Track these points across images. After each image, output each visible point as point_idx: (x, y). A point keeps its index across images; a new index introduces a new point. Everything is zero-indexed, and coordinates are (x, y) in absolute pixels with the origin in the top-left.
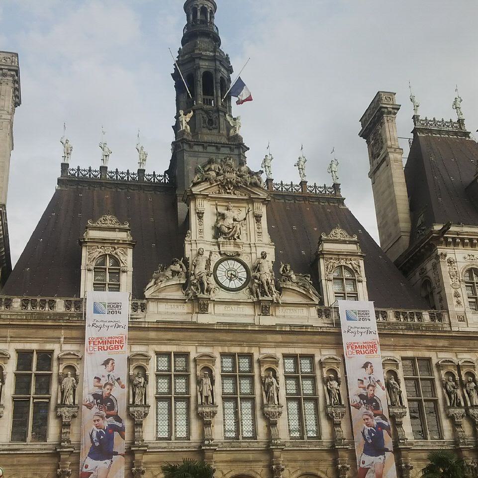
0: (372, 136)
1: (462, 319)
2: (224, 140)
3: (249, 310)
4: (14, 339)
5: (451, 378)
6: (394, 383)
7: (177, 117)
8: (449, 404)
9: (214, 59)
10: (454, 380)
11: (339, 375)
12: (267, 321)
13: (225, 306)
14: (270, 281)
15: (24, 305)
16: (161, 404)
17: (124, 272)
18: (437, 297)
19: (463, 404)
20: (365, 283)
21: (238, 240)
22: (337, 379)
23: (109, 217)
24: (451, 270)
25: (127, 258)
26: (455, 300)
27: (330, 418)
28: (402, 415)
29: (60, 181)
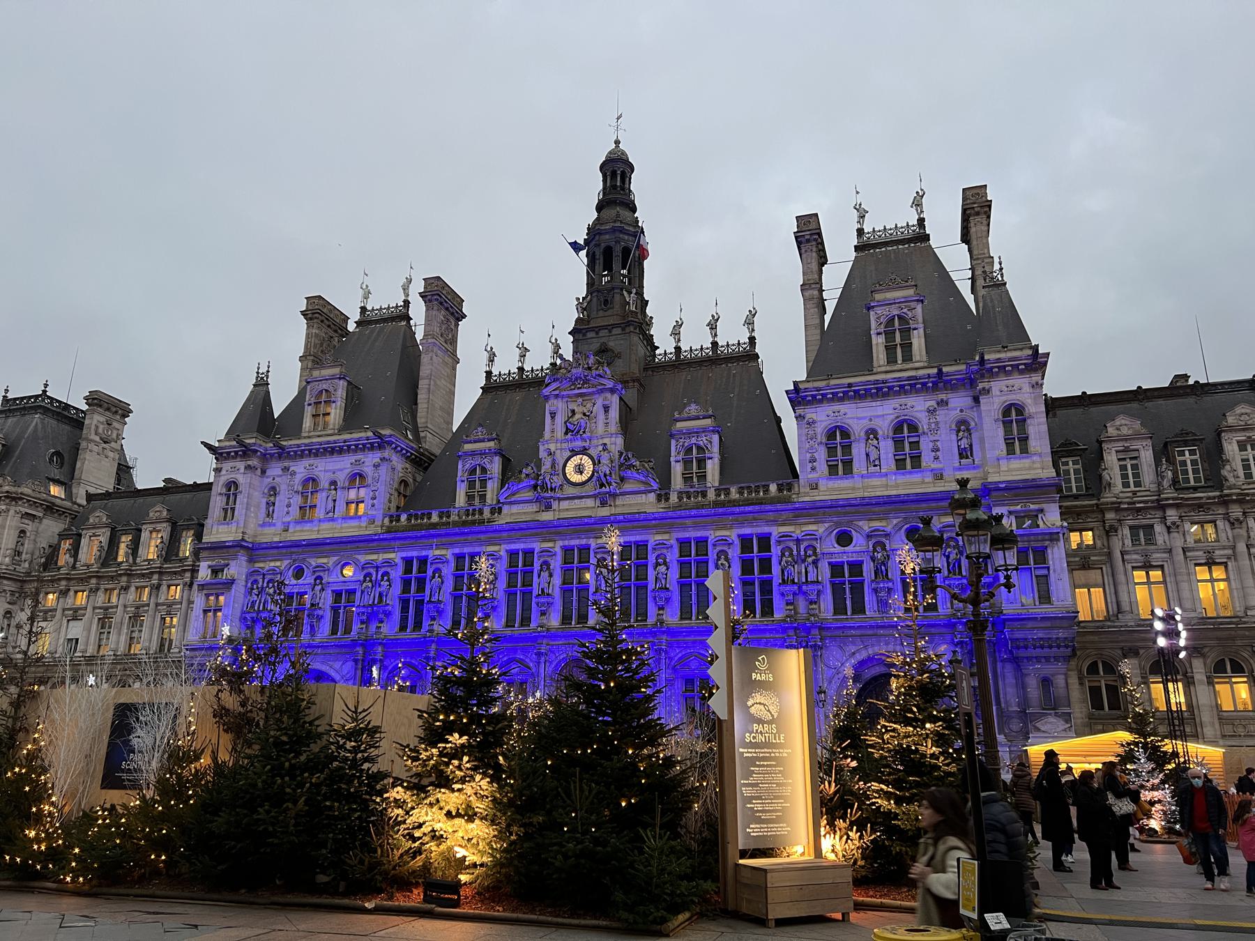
1: (814, 487)
3: (590, 503)
4: (401, 549)
5: (787, 554)
6: (722, 564)
9: (614, 230)
10: (791, 555)
12: (605, 512)
13: (568, 501)
14: (608, 472)
15: (409, 519)
19: (796, 581)
20: (717, 460)
21: (584, 435)
22: (665, 563)
23: (480, 429)
24: (810, 432)
25: (495, 467)
26: (810, 465)
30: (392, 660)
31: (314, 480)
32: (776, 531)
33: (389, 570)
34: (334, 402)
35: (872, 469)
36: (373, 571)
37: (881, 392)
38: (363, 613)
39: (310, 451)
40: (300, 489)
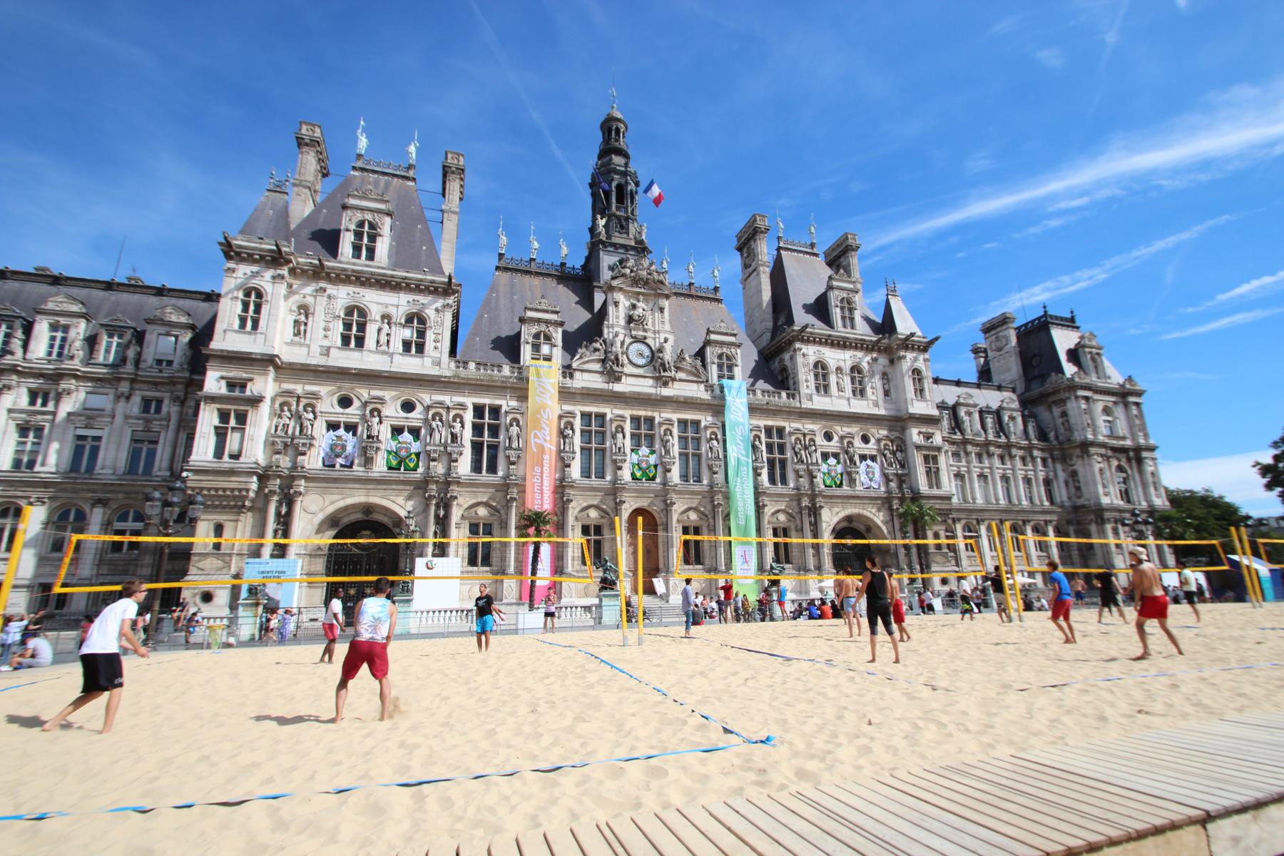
0: (745, 250)
1: (810, 399)
2: (633, 243)
3: (651, 382)
7: (594, 219)
8: (796, 461)
10: (801, 444)
11: (719, 436)
12: (666, 392)
16: (583, 451)
17: (555, 346)
18: (791, 382)
20: (740, 368)
22: (717, 439)
23: (543, 301)
25: (558, 336)
26: (805, 384)
27: (710, 468)
28: (762, 468)
29: (498, 268)
30: (467, 499)
31: (358, 307)
32: (789, 426)
33: (461, 412)
34: (380, 236)
35: (841, 393)
36: (441, 410)
37: (842, 344)
38: (435, 451)
39: (358, 278)
40: (342, 315)
